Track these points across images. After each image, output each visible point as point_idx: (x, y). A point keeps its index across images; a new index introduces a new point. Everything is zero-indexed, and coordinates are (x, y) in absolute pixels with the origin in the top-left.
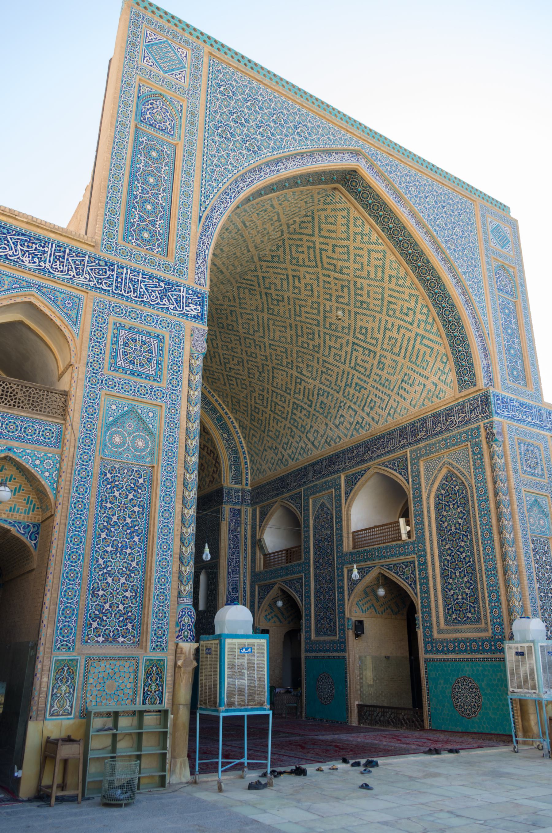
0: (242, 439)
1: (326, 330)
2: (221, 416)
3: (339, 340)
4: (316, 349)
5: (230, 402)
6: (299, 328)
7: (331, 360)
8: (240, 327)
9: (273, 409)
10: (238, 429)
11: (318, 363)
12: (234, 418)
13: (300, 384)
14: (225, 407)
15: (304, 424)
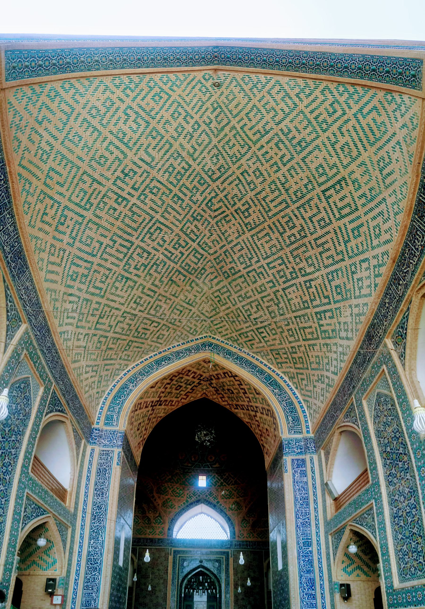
0: (296, 391)
1: (297, 205)
2: (269, 375)
3: (312, 203)
4: (303, 234)
5: (273, 358)
6: (278, 224)
7: (320, 232)
8: (239, 264)
9: (304, 338)
10: (289, 382)
11: (312, 248)
12: (283, 372)
13: (311, 287)
14: (271, 366)
15: (333, 327)
